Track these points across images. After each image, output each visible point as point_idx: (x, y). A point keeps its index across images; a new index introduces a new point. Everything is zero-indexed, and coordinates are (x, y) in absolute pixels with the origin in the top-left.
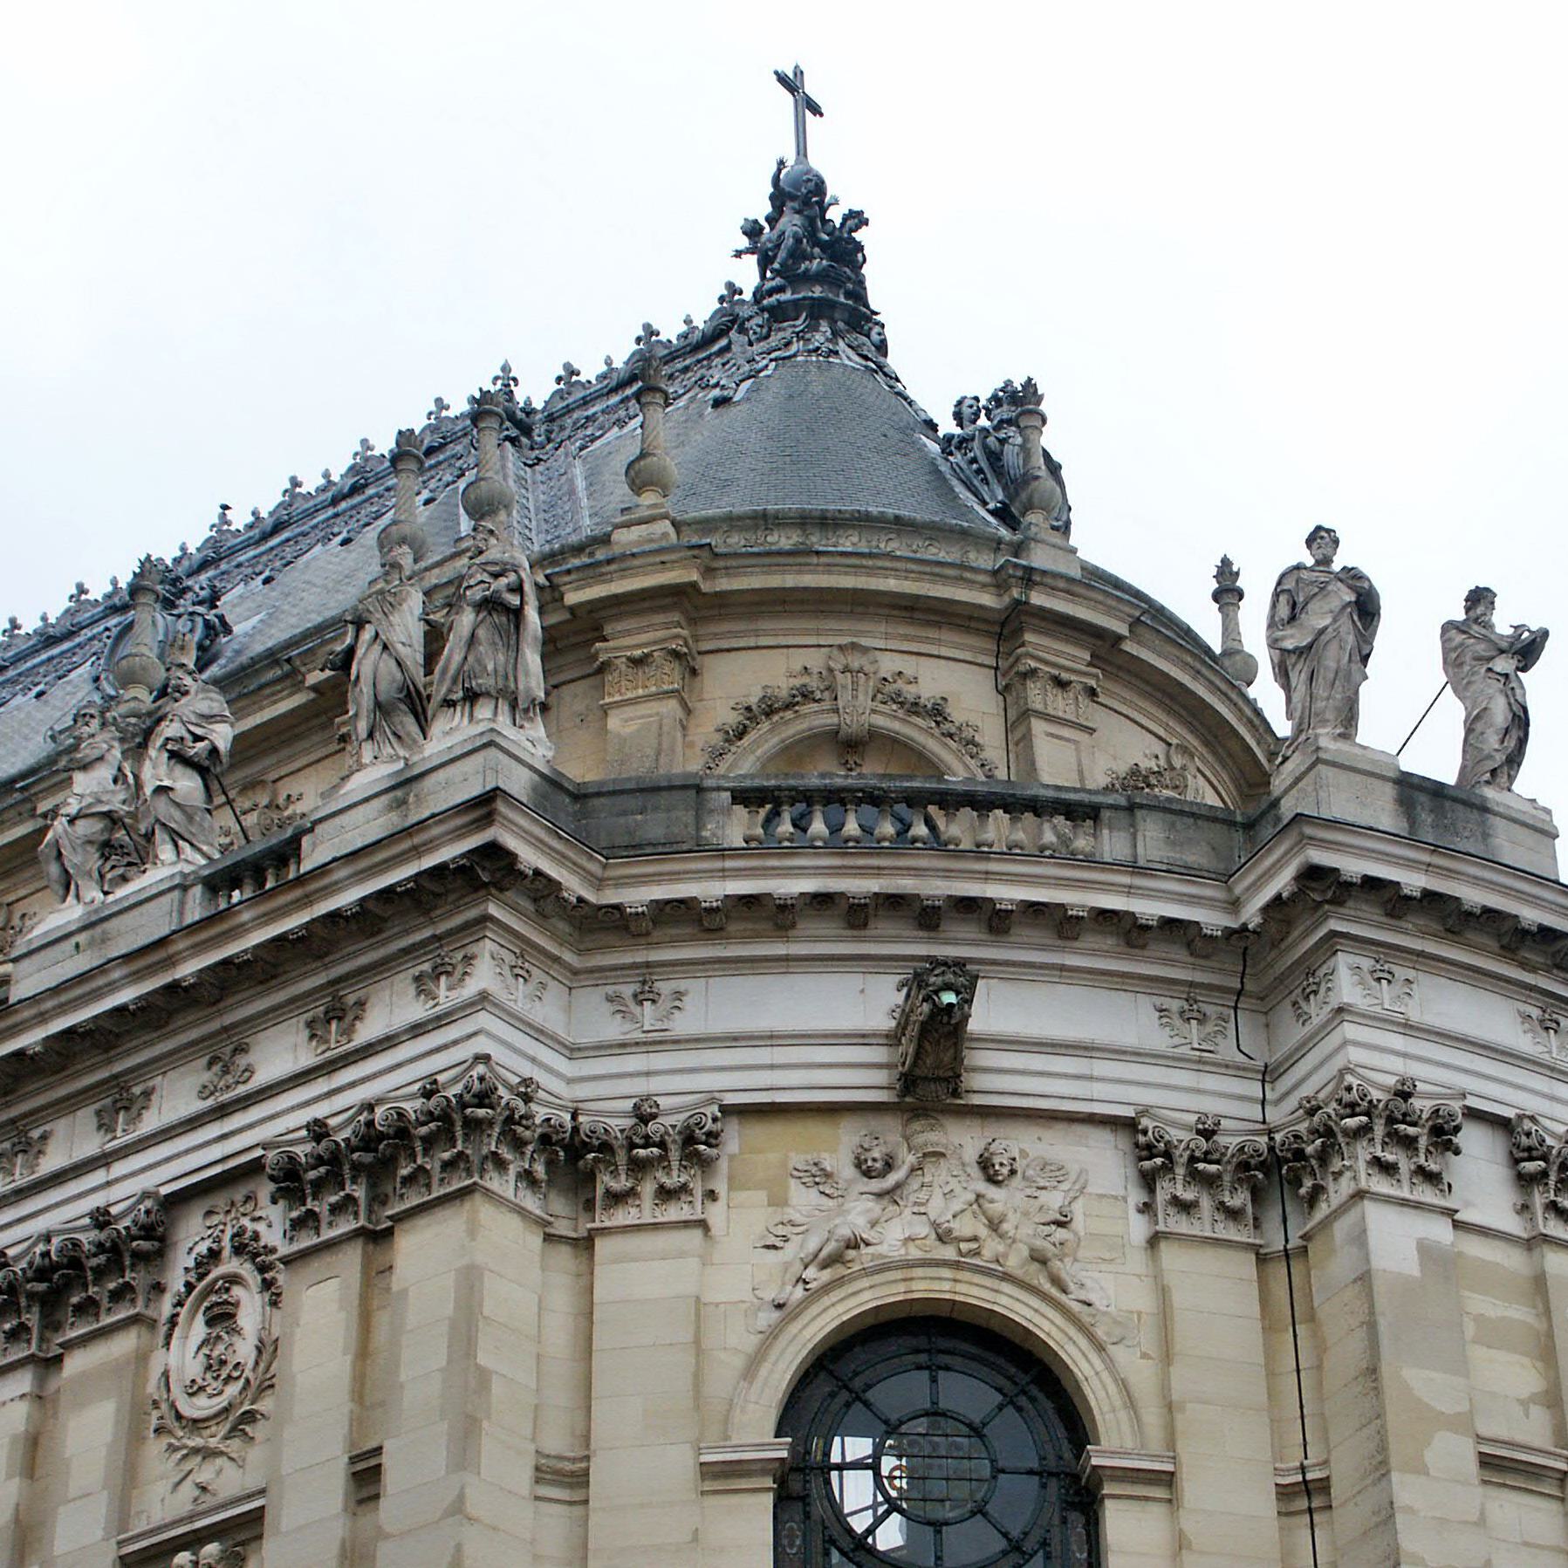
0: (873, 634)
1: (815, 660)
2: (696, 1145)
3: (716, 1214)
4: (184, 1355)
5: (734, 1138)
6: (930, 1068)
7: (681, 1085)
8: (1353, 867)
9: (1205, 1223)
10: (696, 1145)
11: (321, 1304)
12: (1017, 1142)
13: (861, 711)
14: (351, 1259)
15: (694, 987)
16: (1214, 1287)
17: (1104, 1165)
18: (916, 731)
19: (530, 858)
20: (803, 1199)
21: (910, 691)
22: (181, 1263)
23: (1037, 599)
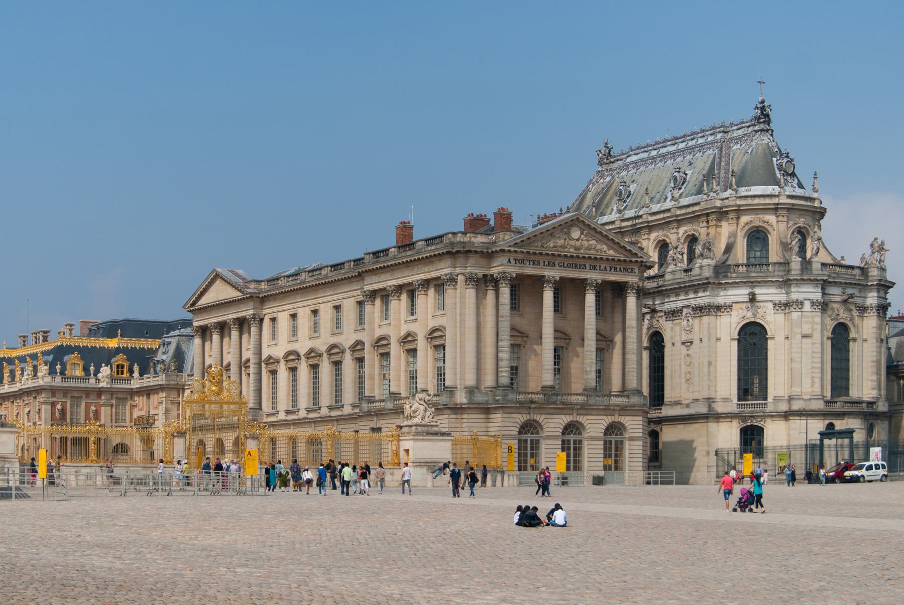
2: (730, 307)
4: (685, 323)
6: (753, 299)
7: (728, 300)
9: (780, 311)
10: (730, 307)
12: (761, 304)
13: (757, 224)
17: (770, 305)
18: (765, 225)
22: (684, 313)
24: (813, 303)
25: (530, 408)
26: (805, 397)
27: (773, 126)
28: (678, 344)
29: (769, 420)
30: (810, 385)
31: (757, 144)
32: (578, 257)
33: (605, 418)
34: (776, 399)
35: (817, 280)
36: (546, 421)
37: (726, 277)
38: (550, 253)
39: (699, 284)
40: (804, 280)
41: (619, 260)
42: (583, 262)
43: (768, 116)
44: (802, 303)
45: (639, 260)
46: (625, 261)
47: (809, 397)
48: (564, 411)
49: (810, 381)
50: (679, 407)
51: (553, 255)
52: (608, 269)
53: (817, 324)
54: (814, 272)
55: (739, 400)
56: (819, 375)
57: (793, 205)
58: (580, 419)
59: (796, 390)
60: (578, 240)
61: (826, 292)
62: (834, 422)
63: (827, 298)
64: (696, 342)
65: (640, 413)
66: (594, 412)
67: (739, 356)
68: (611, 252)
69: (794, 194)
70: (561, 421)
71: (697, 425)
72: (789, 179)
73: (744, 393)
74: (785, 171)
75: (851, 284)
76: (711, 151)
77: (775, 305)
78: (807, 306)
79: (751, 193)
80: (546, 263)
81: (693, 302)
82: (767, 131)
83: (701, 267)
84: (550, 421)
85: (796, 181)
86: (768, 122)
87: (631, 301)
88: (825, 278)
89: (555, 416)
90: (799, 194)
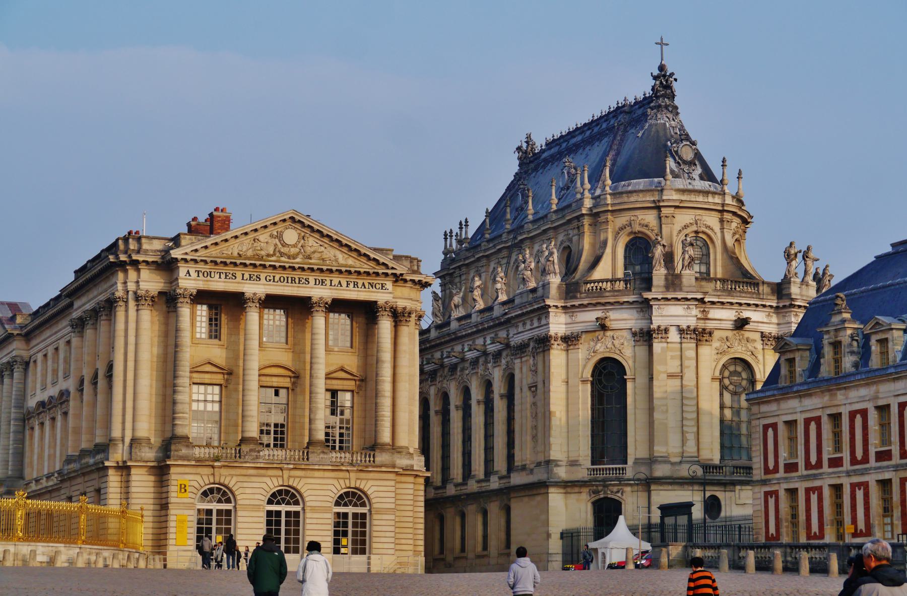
0: (638, 213)
1: (628, 218)
3: (580, 346)
5: (584, 336)
8: (650, 297)
11: (540, 358)
14: (542, 354)
15: (578, 314)
16: (642, 351)
17: (627, 335)
19: (551, 304)
20: (592, 343)
21: (642, 222)
23: (661, 204)
24: (681, 331)
25: (213, 467)
26: (673, 460)
27: (677, 102)
28: (525, 389)
29: (628, 489)
30: (679, 444)
31: (650, 125)
32: (293, 268)
33: (335, 482)
34: (637, 461)
35: (687, 299)
36: (239, 485)
37: (575, 297)
38: (248, 262)
39: (538, 309)
40: (667, 299)
41: (359, 273)
42: (304, 275)
43: (668, 87)
44: (666, 331)
45: (390, 272)
46: (368, 274)
47: (678, 460)
48: (270, 472)
49: (678, 437)
50: (524, 473)
51: (255, 266)
52: (344, 284)
53: (689, 359)
54: (685, 289)
55: (593, 463)
56: (695, 429)
57: (682, 201)
58: (294, 483)
59: (659, 450)
60: (295, 246)
61: (710, 316)
62: (718, 494)
63: (710, 325)
64: (540, 386)
65: (392, 476)
66: (317, 474)
67: (592, 405)
68: (350, 262)
69: (690, 187)
70: (264, 485)
71: (539, 498)
72: (686, 168)
73: (597, 457)
74: (680, 158)
75: (749, 305)
76: (606, 139)
77: (634, 334)
78: (674, 336)
79: (630, 188)
80: (247, 276)
81: (536, 333)
82: (666, 107)
83: (544, 286)
84: (245, 485)
85: (699, 170)
86: (672, 96)
87: (385, 325)
88: (699, 296)
89: (254, 479)
90: (700, 188)
